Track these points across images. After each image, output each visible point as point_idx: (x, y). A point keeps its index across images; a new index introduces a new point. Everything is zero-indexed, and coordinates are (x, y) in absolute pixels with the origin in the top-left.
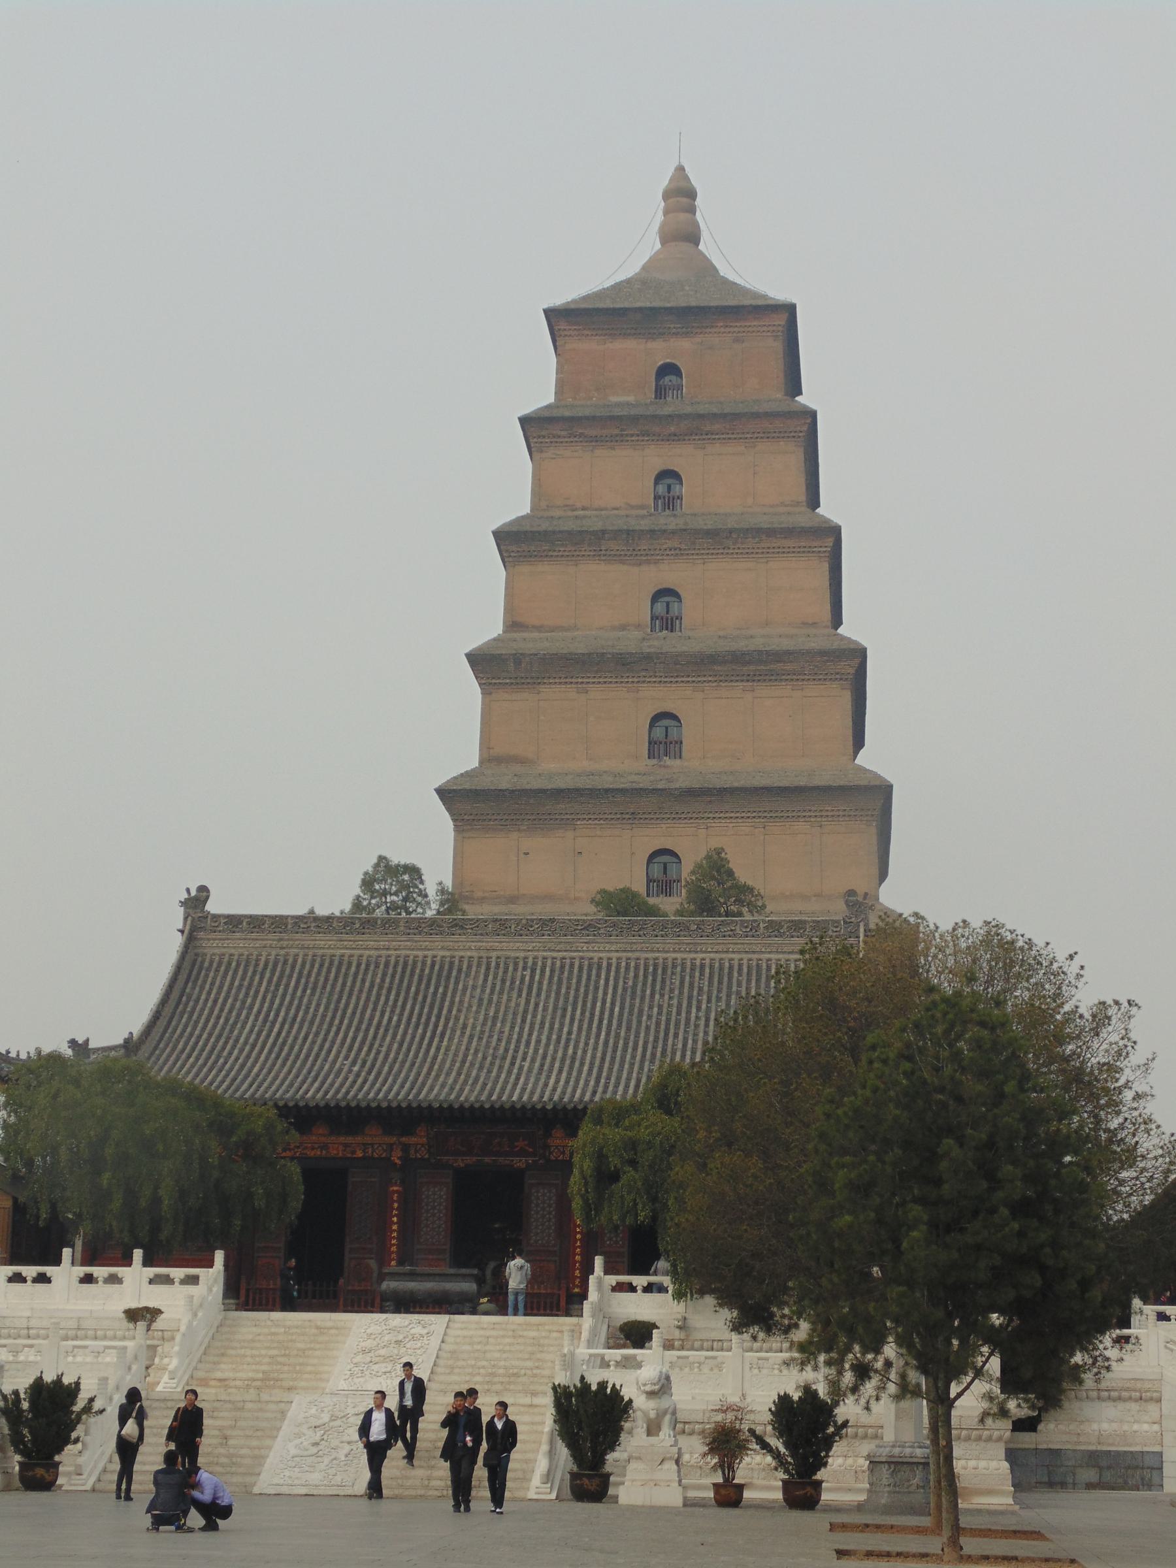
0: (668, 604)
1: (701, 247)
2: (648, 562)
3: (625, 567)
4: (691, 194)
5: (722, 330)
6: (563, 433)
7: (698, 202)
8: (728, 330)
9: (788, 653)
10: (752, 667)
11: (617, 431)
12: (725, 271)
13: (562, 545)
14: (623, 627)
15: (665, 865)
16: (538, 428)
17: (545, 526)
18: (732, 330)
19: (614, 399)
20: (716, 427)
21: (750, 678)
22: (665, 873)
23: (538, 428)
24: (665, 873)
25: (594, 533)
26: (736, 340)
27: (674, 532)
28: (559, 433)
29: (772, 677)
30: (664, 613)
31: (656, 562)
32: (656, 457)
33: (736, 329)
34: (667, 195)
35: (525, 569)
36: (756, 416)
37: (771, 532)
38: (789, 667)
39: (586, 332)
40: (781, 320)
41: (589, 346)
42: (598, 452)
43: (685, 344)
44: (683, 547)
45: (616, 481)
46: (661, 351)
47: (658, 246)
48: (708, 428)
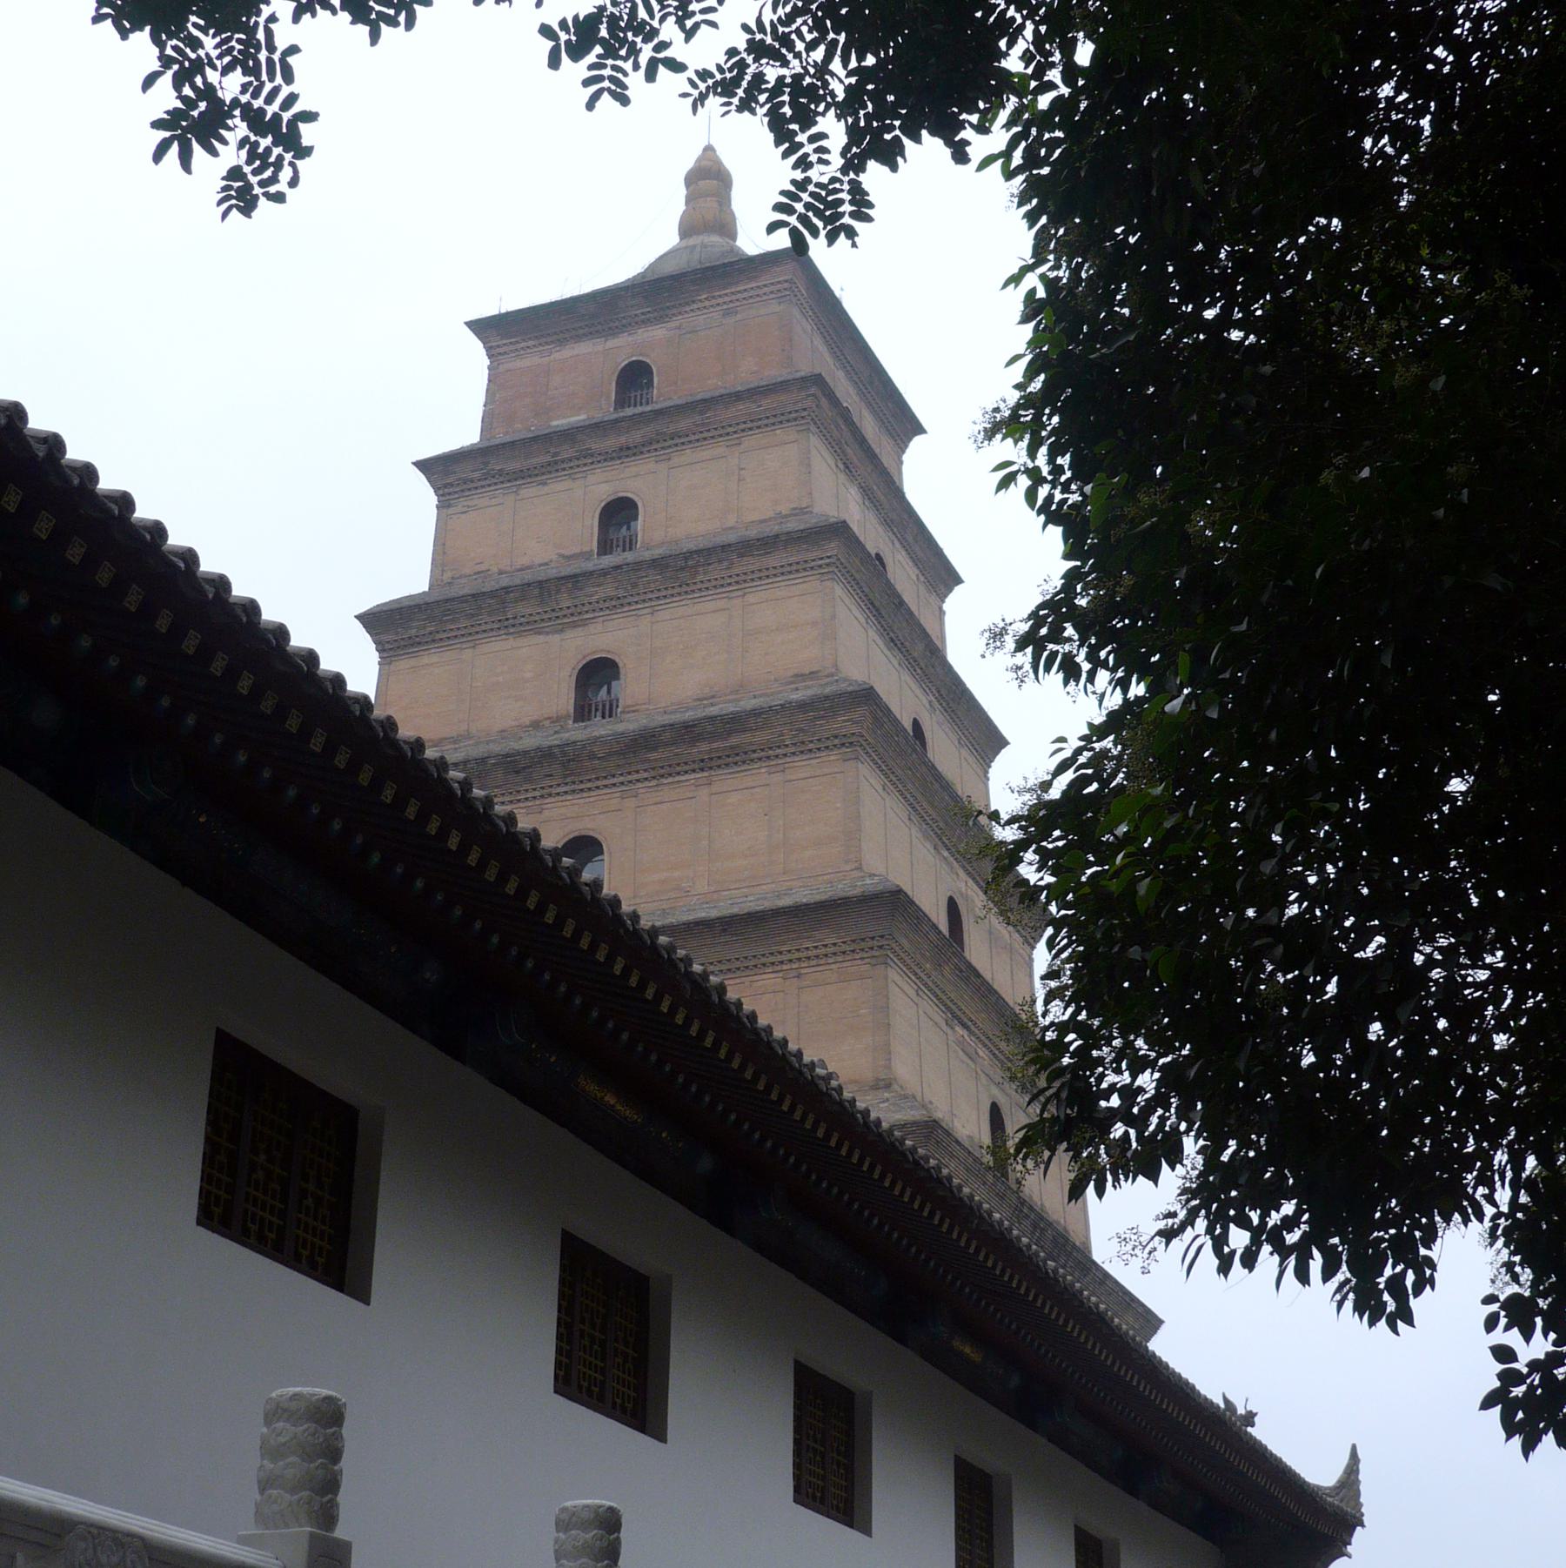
2: (574, 625)
3: (541, 638)
5: (707, 303)
6: (477, 475)
8: (714, 302)
9: (756, 713)
10: (704, 747)
11: (549, 458)
13: (453, 621)
14: (536, 725)
18: (720, 300)
19: (555, 423)
20: (684, 424)
21: (704, 765)
25: (492, 594)
26: (727, 313)
27: (604, 573)
28: (471, 475)
29: (738, 758)
31: (584, 623)
32: (600, 486)
33: (727, 299)
35: (404, 664)
36: (738, 396)
37: (746, 547)
38: (761, 737)
39: (523, 344)
41: (530, 360)
42: (524, 492)
43: (658, 332)
44: (621, 593)
46: (622, 348)
48: (672, 429)
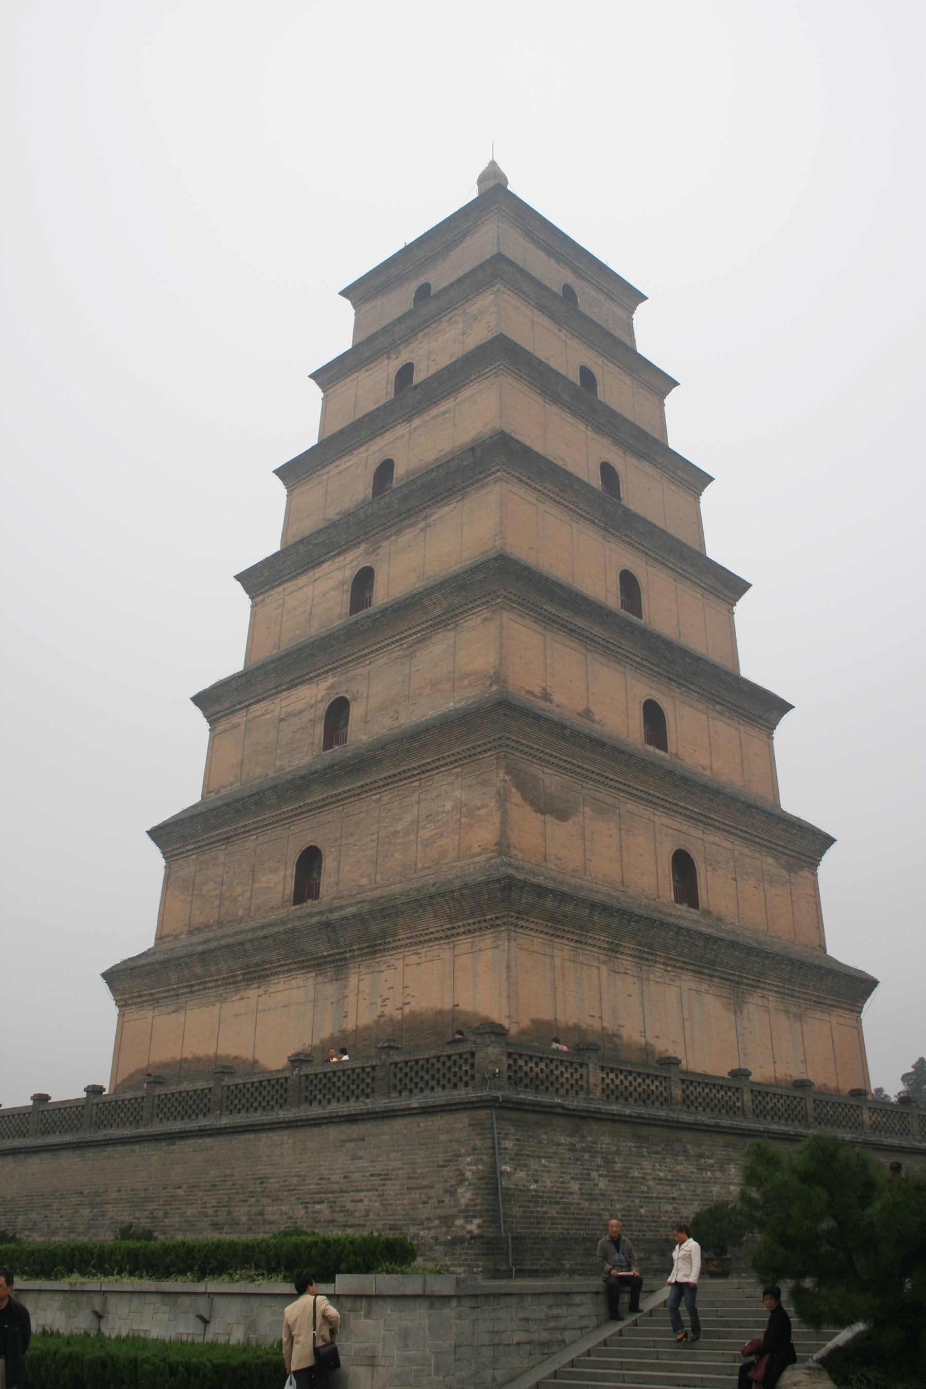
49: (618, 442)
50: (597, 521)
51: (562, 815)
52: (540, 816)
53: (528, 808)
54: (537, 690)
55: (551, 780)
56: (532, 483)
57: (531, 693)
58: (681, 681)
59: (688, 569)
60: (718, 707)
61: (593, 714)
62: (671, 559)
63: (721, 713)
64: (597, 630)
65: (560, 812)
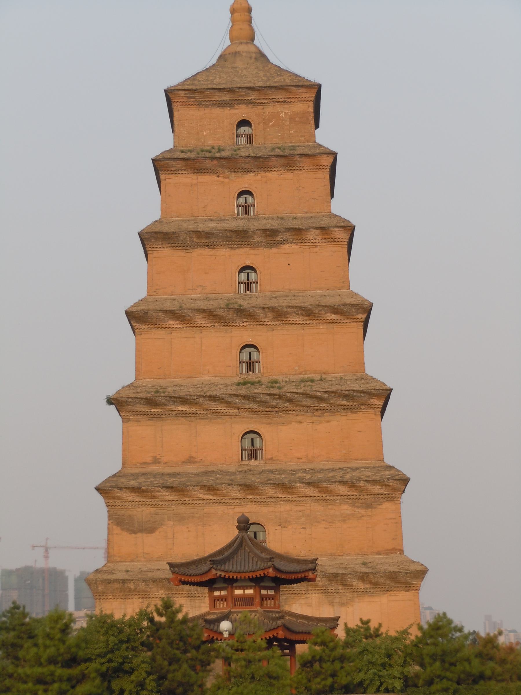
0: (248, 274)
1: (256, 42)
4: (250, 10)
7: (253, 14)
12: (273, 59)
15: (252, 439)
16: (163, 165)
17: (173, 228)
22: (253, 445)
23: (163, 165)
24: (253, 445)
30: (246, 281)
34: (233, 11)
40: (312, 94)
45: (213, 198)
47: (229, 43)
49: (256, 245)
50: (216, 325)
51: (151, 530)
52: (134, 535)
53: (125, 533)
54: (149, 460)
55: (141, 514)
56: (159, 326)
57: (145, 463)
58: (277, 409)
59: (307, 318)
60: (319, 412)
61: (194, 458)
62: (288, 319)
63: (322, 415)
64: (195, 407)
65: (150, 529)
